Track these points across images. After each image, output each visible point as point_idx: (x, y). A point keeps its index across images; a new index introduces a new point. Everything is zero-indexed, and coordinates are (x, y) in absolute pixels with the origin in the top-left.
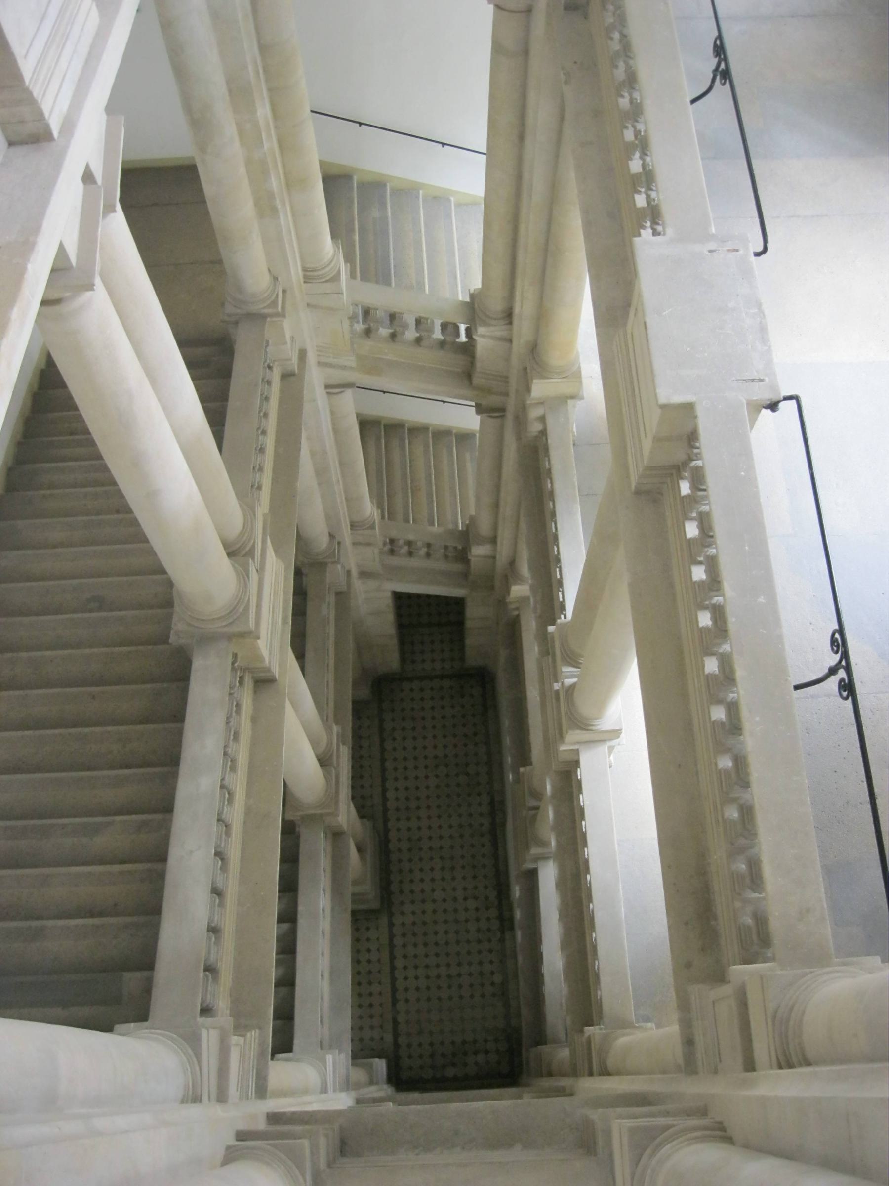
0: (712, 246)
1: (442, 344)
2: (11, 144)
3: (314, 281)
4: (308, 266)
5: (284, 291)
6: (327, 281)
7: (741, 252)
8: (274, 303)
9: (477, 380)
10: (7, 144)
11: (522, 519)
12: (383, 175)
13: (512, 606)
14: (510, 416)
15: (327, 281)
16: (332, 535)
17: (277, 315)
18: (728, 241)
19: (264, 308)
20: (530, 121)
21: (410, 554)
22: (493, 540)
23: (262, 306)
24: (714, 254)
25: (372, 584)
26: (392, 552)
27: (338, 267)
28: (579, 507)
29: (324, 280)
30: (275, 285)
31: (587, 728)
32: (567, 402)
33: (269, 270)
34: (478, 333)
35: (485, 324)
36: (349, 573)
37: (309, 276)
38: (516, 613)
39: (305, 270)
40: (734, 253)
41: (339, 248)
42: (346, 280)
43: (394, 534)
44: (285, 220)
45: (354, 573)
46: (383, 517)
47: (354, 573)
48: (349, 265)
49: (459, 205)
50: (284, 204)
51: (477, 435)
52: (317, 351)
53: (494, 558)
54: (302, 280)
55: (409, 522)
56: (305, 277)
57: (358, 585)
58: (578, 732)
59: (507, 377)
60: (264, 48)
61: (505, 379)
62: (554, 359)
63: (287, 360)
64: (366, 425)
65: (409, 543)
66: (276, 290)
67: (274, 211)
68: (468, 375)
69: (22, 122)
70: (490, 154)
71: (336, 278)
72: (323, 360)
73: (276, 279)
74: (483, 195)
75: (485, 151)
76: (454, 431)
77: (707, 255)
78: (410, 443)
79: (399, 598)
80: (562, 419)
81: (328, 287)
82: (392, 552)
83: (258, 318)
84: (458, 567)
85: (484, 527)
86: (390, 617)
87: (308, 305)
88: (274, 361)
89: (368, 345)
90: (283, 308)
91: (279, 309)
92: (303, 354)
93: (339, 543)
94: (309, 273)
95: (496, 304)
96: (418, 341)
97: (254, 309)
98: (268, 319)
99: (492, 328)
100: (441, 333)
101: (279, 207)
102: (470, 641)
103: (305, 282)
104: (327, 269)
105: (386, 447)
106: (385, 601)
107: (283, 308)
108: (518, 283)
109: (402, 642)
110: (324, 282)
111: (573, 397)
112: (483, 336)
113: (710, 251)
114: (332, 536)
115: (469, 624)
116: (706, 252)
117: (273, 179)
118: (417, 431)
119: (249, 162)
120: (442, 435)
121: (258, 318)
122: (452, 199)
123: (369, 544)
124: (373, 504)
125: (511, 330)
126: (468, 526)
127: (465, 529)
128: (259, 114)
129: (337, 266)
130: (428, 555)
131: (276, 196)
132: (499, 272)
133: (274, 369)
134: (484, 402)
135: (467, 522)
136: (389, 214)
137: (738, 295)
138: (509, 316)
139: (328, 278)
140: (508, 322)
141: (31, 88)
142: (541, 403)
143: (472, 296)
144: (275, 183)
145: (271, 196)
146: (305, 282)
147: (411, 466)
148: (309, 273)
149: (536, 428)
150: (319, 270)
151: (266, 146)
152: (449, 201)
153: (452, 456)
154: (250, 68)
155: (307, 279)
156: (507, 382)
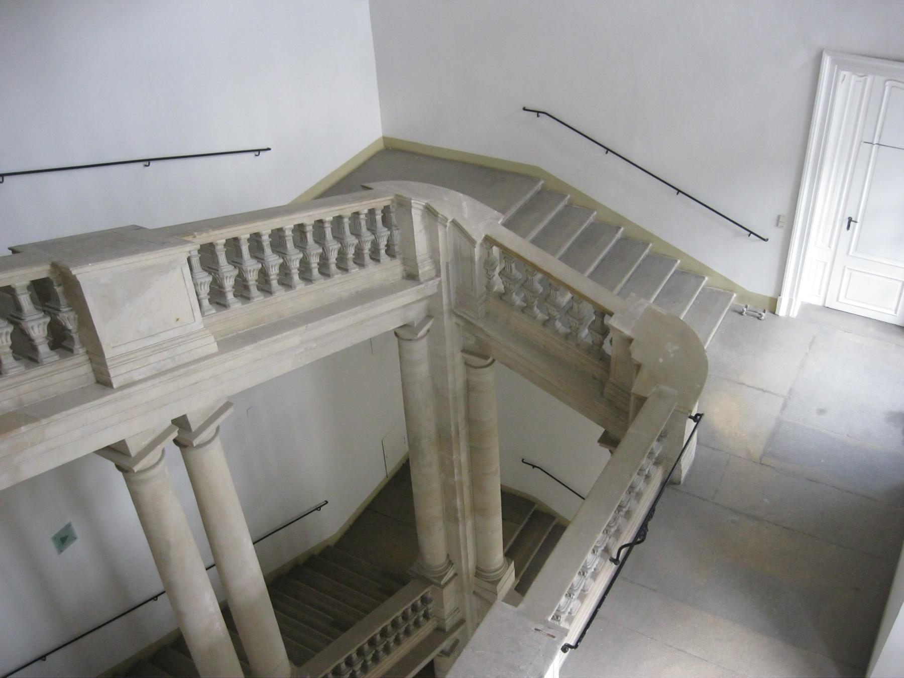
0: (540, 627)
2: (98, 382)
5: (456, 574)
6: (488, 582)
7: (555, 639)
8: (442, 577)
10: (95, 381)
18: (553, 629)
19: (433, 577)
23: (432, 576)
24: (538, 632)
27: (500, 577)
29: (486, 580)
30: (447, 568)
33: (448, 556)
37: (480, 572)
39: (477, 568)
40: (551, 638)
41: (509, 565)
44: (467, 528)
56: (476, 573)
60: (470, 421)
66: (447, 571)
67: (456, 520)
69: (102, 374)
71: (496, 582)
73: (450, 563)
77: (532, 631)
81: (488, 586)
83: (427, 582)
87: (474, 592)
88: (434, 616)
90: (446, 584)
91: (442, 583)
98: (433, 586)
104: (492, 574)
107: (446, 584)
110: (486, 581)
113: (536, 630)
116: (533, 629)
121: (427, 582)
128: (454, 457)
129: (499, 576)
131: (459, 510)
133: (430, 621)
137: (531, 664)
141: (107, 360)
144: (463, 502)
145: (456, 510)
146: (475, 576)
150: (486, 572)
151: (456, 478)
154: (453, 428)
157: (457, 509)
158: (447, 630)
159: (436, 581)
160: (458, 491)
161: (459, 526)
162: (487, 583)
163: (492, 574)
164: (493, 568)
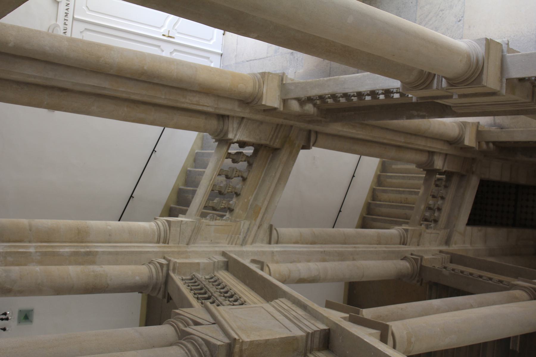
1: (250, 165)
3: (168, 238)
4: (156, 239)
8: (161, 265)
9: (277, 144)
11: (366, 122)
12: (173, 189)
13: (484, 146)
14: (311, 127)
15: (170, 230)
16: (404, 258)
17: (168, 265)
20: (124, 95)
21: (439, 209)
22: (431, 153)
23: (161, 274)
25: (456, 237)
26: (436, 221)
28: (342, 76)
31: (481, 68)
32: (284, 84)
34: (233, 138)
35: (226, 133)
36: (441, 252)
38: (491, 145)
39: (158, 242)
42: (185, 218)
43: (418, 218)
45: (444, 248)
46: (407, 223)
47: (444, 248)
48: (180, 215)
49: (202, 148)
50: (88, 247)
51: (384, 160)
52: (232, 244)
53: (446, 155)
54: (166, 245)
55: (413, 207)
56: (164, 242)
57: (456, 247)
58: (484, 77)
59: (278, 125)
61: (279, 126)
62: (248, 88)
63: (214, 265)
64: (364, 224)
65: (429, 208)
68: (274, 151)
70: (165, 125)
72: (240, 241)
74: (197, 133)
75: (163, 128)
76: (379, 173)
78: (380, 201)
79: (472, 221)
80: (292, 87)
82: (436, 221)
84: (455, 180)
85: (423, 158)
86: (490, 230)
87: (188, 244)
89: (237, 210)
92: (224, 254)
93: (412, 254)
94: (162, 240)
95: (214, 123)
96: (244, 179)
97: (161, 279)
99: (230, 129)
100: (237, 163)
101: (88, 250)
102: (522, 181)
103: (168, 244)
104: (162, 228)
105: (379, 216)
106: (476, 231)
108: (185, 106)
109: (525, 226)
111: (282, 80)
112: (236, 135)
114: (404, 258)
115: (506, 178)
117: (61, 250)
118: (374, 194)
119: (40, 263)
120: (379, 180)
122: (196, 151)
123: (420, 235)
124: (393, 228)
125: (233, 117)
126: (424, 170)
127: (425, 172)
129: (163, 222)
130: (443, 198)
132: (201, 121)
134: (303, 143)
135: (422, 170)
136: (192, 188)
138: (222, 117)
139: (168, 228)
140: (227, 118)
142: (285, 101)
143: (216, 141)
146: (168, 244)
147: (393, 202)
148: (162, 240)
149: (310, 108)
151: (32, 250)
152: (197, 153)
153: (392, 176)
155: (166, 241)
156: (282, 125)
157: (74, 252)
158: (226, 260)
159: (165, 269)
160: (50, 250)
161: (97, 252)
162: (172, 231)
163: (162, 228)
164: (155, 228)
